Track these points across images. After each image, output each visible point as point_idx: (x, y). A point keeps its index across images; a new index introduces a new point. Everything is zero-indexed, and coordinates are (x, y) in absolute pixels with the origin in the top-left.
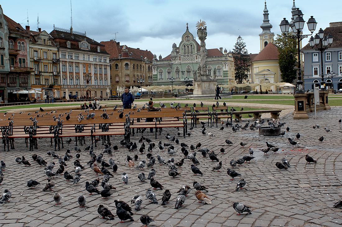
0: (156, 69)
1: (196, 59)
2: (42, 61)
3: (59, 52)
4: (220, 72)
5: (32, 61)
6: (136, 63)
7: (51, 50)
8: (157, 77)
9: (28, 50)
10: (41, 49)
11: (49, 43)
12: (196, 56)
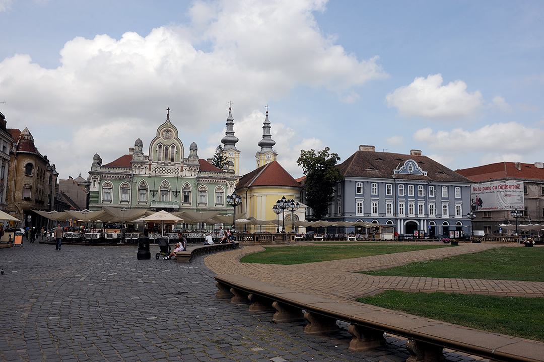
0: (98, 181)
1: (179, 171)
4: (221, 197)
8: (98, 197)
12: (182, 167)
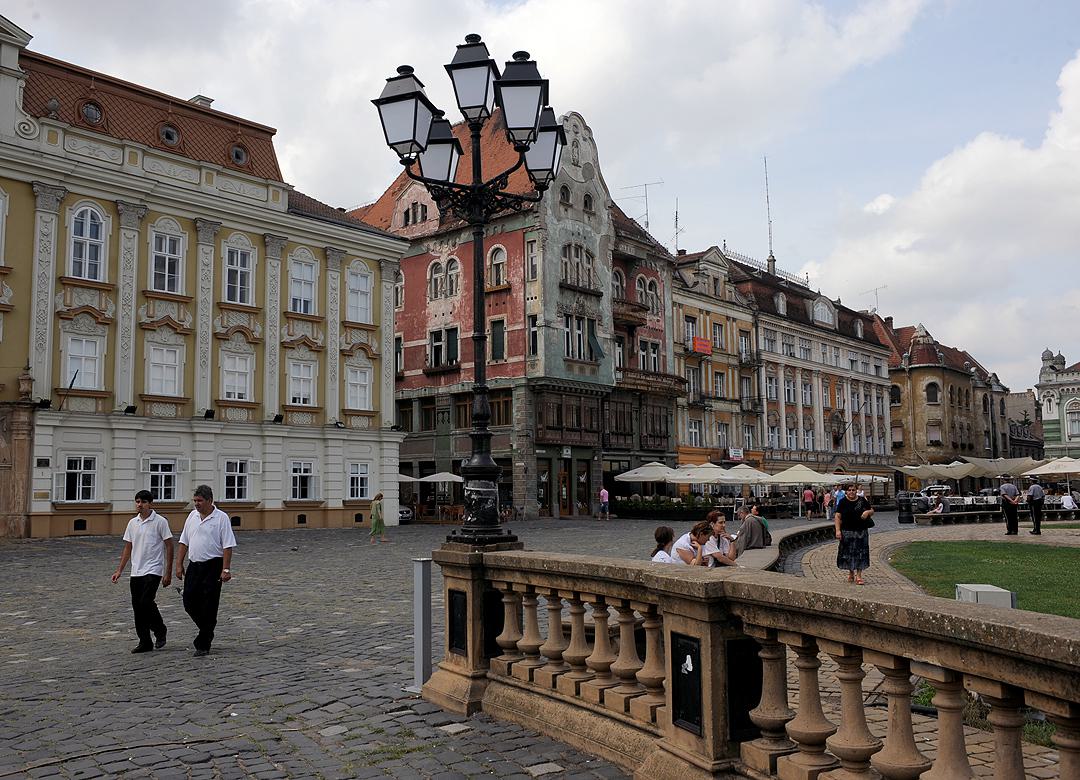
0: (1055, 401)
3: (757, 328)
6: (959, 383)
7: (734, 320)
8: (1059, 430)
9: (668, 313)
10: (708, 313)
11: (729, 292)
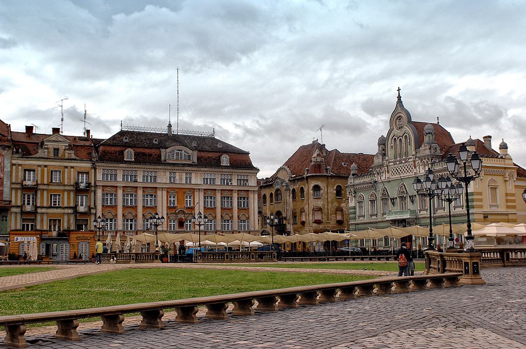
1: (414, 168)
2: (71, 188)
3: (95, 169)
5: (16, 189)
9: (7, 169)
10: (46, 166)
12: (414, 161)
